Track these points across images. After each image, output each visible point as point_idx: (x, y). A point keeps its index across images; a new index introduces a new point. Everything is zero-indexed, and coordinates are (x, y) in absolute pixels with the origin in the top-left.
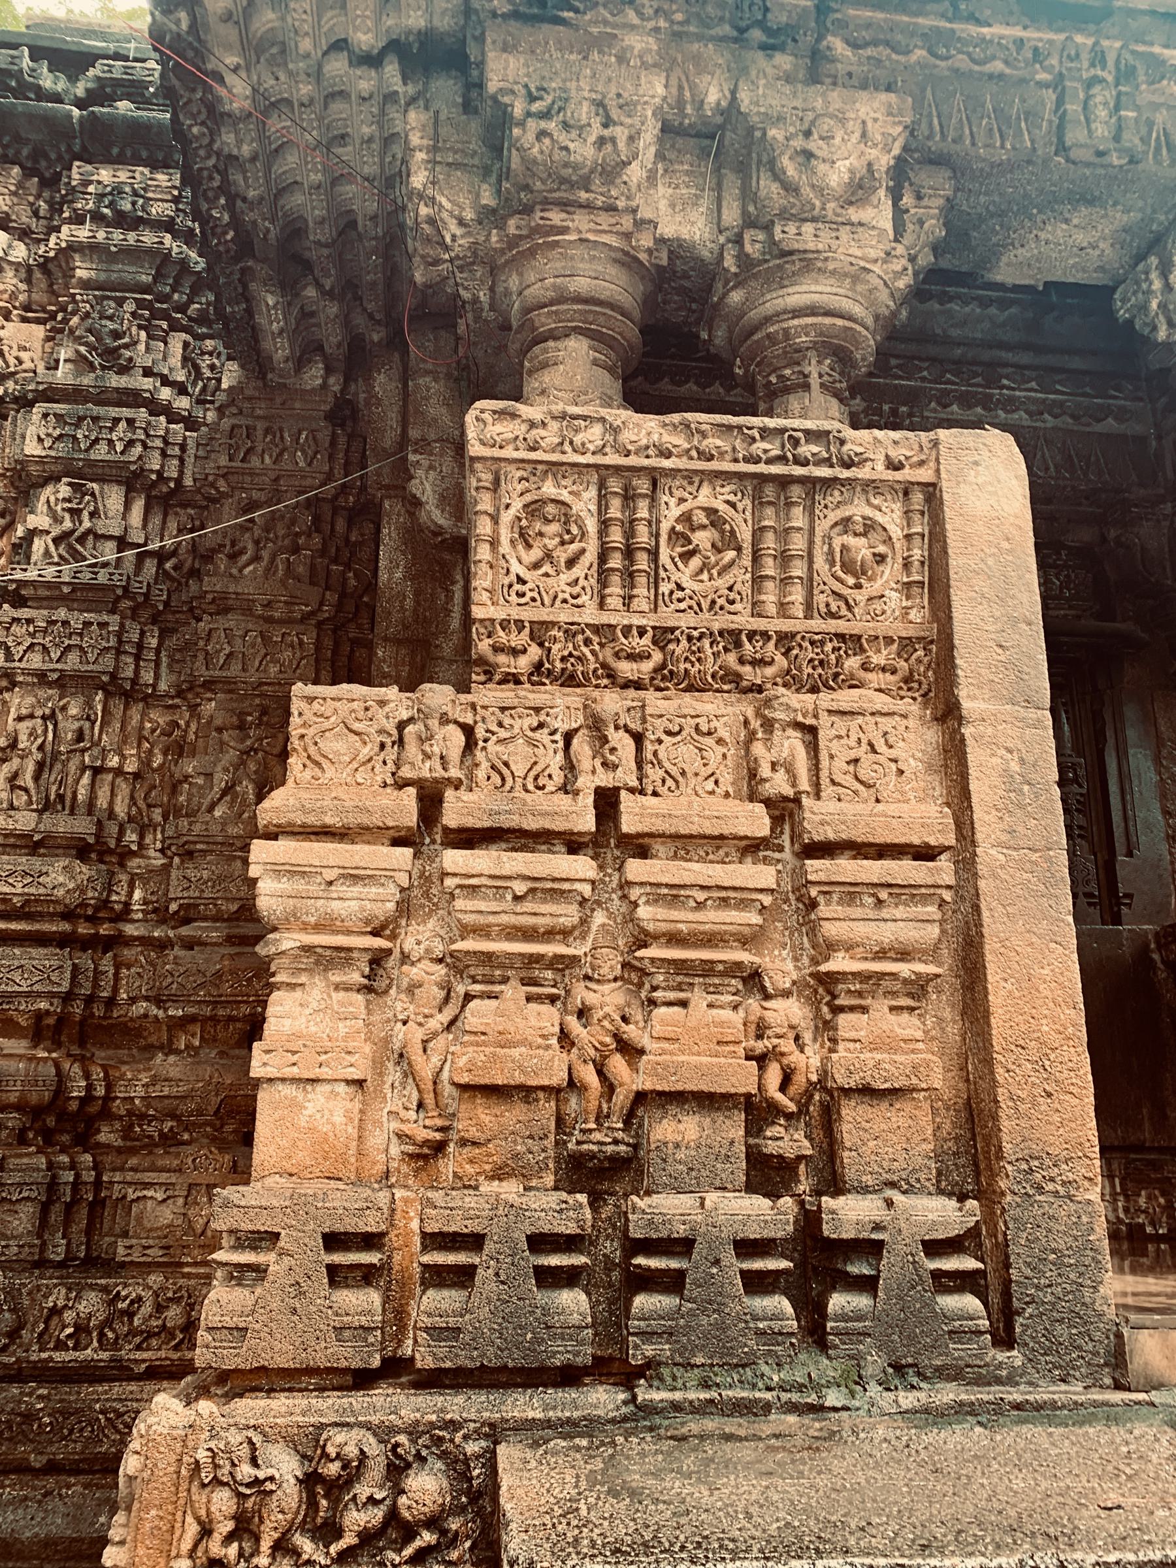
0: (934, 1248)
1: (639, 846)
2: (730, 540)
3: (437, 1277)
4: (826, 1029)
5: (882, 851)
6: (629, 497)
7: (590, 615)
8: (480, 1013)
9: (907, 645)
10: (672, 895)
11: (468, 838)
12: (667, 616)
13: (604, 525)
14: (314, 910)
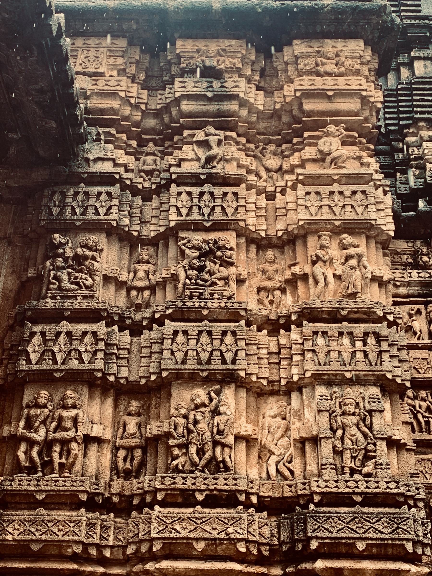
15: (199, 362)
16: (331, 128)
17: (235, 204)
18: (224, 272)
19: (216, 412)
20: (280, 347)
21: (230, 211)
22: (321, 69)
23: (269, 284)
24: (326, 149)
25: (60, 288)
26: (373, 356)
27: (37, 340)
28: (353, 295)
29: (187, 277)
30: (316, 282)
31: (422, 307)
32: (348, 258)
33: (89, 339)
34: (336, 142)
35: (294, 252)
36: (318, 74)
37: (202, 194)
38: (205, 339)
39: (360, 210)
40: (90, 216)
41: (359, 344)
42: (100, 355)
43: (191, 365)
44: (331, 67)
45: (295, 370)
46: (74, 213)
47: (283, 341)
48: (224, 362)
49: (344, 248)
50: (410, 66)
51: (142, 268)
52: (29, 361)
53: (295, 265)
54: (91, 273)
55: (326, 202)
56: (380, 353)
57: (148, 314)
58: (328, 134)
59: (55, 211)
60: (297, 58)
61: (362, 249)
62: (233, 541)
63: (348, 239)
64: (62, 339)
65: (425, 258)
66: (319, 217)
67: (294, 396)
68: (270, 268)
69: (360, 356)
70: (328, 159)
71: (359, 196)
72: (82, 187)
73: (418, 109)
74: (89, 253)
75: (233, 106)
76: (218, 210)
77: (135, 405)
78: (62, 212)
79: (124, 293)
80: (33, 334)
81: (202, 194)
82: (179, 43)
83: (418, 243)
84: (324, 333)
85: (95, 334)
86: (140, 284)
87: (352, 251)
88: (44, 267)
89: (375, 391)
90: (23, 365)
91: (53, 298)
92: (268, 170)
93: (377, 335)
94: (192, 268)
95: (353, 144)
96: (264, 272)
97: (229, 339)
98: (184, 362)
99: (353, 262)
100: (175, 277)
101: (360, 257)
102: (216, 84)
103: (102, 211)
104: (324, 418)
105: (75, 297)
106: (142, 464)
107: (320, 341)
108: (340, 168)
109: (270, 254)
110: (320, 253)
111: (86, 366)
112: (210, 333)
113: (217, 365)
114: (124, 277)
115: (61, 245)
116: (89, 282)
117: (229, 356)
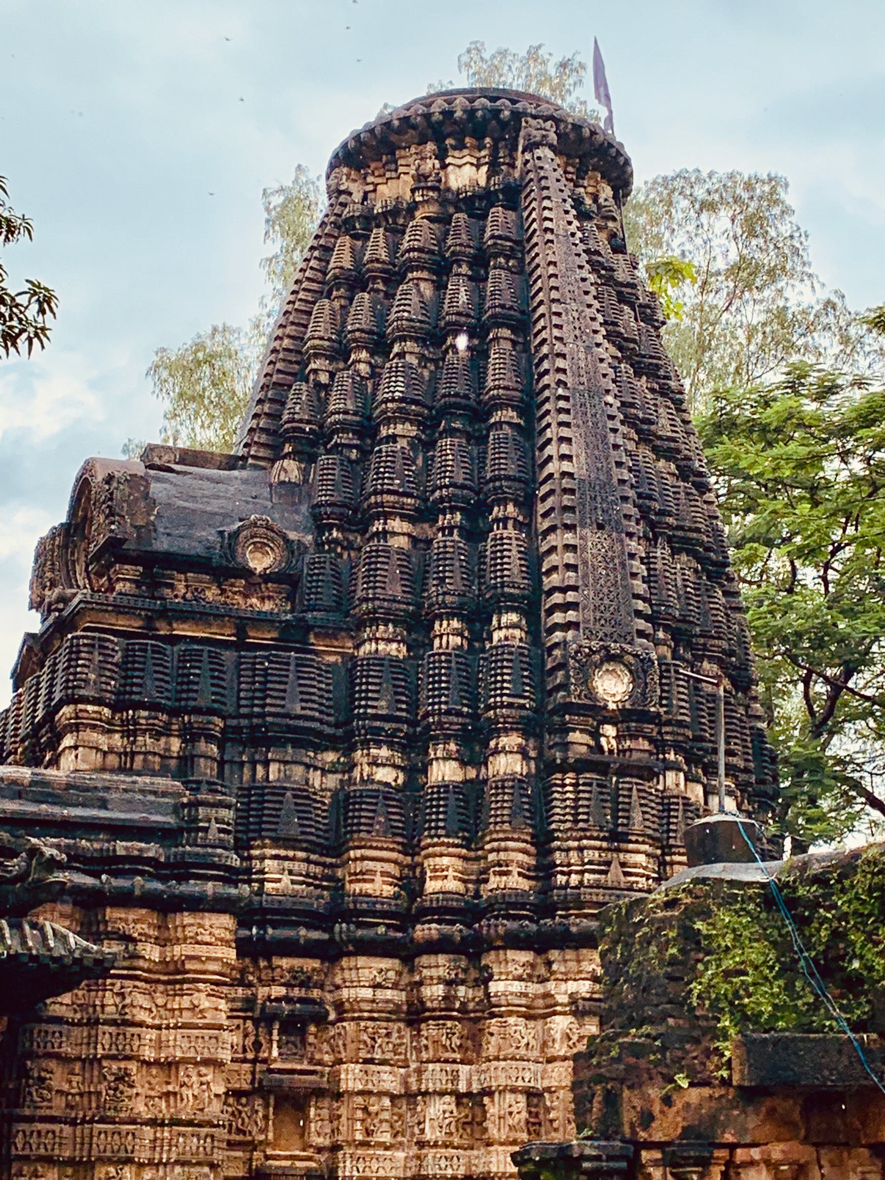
15: (113, 1152)
16: (201, 986)
17: (137, 1043)
20: (155, 1139)
21: (135, 1048)
22: (199, 938)
23: (153, 1093)
24: (196, 1002)
25: (32, 1101)
26: (208, 1149)
27: (21, 1134)
28: (202, 1110)
29: (107, 1094)
30: (182, 1100)
31: (241, 1021)
32: (202, 1084)
33: (50, 1135)
34: (203, 995)
35: (170, 1070)
36: (198, 943)
37: (118, 1034)
38: (116, 1137)
39: (212, 1050)
40: (49, 1049)
41: (202, 1142)
42: (56, 1146)
43: (108, 1154)
44: (207, 938)
45: (165, 1156)
46: (39, 1046)
47: (158, 1135)
48: (126, 1151)
49: (201, 1076)
50: (266, 764)
51: (76, 1079)
52: (17, 1149)
53: (168, 1083)
54: (50, 1090)
55: (193, 1044)
56: (213, 1148)
58: (199, 991)
59: (27, 1044)
60: (184, 927)
61: (209, 1078)
63: (203, 1070)
64: (35, 1134)
65: (251, 978)
66: (188, 1055)
67: (161, 1168)
68: (153, 1081)
69: (201, 1149)
70: (197, 1010)
71: (214, 1041)
72: (44, 1026)
73: (275, 678)
74: (48, 1076)
75: (141, 963)
76: (128, 1047)
78: (32, 1045)
79: (64, 1098)
80: (18, 1132)
81: (118, 1034)
82: (108, 910)
83: (247, 960)
84: (184, 1135)
85: (54, 1132)
86: (73, 1091)
87: (204, 1079)
88: (20, 1084)
89: (206, 1170)
91: (29, 1107)
92: (157, 1006)
93: (212, 1137)
94: (110, 1088)
95: (213, 995)
96: (150, 1083)
97: (130, 1137)
98: (105, 1151)
99: (205, 1087)
100: (99, 1094)
101: (208, 1083)
102: (131, 947)
103: (56, 1045)
105: (41, 1108)
107: (181, 1140)
108: (205, 1017)
109: (154, 1071)
110: (186, 1080)
111: (49, 1153)
112: (119, 1133)
113: (123, 1154)
114: (66, 1087)
115: (31, 1069)
116: (49, 1097)
117: (130, 1148)
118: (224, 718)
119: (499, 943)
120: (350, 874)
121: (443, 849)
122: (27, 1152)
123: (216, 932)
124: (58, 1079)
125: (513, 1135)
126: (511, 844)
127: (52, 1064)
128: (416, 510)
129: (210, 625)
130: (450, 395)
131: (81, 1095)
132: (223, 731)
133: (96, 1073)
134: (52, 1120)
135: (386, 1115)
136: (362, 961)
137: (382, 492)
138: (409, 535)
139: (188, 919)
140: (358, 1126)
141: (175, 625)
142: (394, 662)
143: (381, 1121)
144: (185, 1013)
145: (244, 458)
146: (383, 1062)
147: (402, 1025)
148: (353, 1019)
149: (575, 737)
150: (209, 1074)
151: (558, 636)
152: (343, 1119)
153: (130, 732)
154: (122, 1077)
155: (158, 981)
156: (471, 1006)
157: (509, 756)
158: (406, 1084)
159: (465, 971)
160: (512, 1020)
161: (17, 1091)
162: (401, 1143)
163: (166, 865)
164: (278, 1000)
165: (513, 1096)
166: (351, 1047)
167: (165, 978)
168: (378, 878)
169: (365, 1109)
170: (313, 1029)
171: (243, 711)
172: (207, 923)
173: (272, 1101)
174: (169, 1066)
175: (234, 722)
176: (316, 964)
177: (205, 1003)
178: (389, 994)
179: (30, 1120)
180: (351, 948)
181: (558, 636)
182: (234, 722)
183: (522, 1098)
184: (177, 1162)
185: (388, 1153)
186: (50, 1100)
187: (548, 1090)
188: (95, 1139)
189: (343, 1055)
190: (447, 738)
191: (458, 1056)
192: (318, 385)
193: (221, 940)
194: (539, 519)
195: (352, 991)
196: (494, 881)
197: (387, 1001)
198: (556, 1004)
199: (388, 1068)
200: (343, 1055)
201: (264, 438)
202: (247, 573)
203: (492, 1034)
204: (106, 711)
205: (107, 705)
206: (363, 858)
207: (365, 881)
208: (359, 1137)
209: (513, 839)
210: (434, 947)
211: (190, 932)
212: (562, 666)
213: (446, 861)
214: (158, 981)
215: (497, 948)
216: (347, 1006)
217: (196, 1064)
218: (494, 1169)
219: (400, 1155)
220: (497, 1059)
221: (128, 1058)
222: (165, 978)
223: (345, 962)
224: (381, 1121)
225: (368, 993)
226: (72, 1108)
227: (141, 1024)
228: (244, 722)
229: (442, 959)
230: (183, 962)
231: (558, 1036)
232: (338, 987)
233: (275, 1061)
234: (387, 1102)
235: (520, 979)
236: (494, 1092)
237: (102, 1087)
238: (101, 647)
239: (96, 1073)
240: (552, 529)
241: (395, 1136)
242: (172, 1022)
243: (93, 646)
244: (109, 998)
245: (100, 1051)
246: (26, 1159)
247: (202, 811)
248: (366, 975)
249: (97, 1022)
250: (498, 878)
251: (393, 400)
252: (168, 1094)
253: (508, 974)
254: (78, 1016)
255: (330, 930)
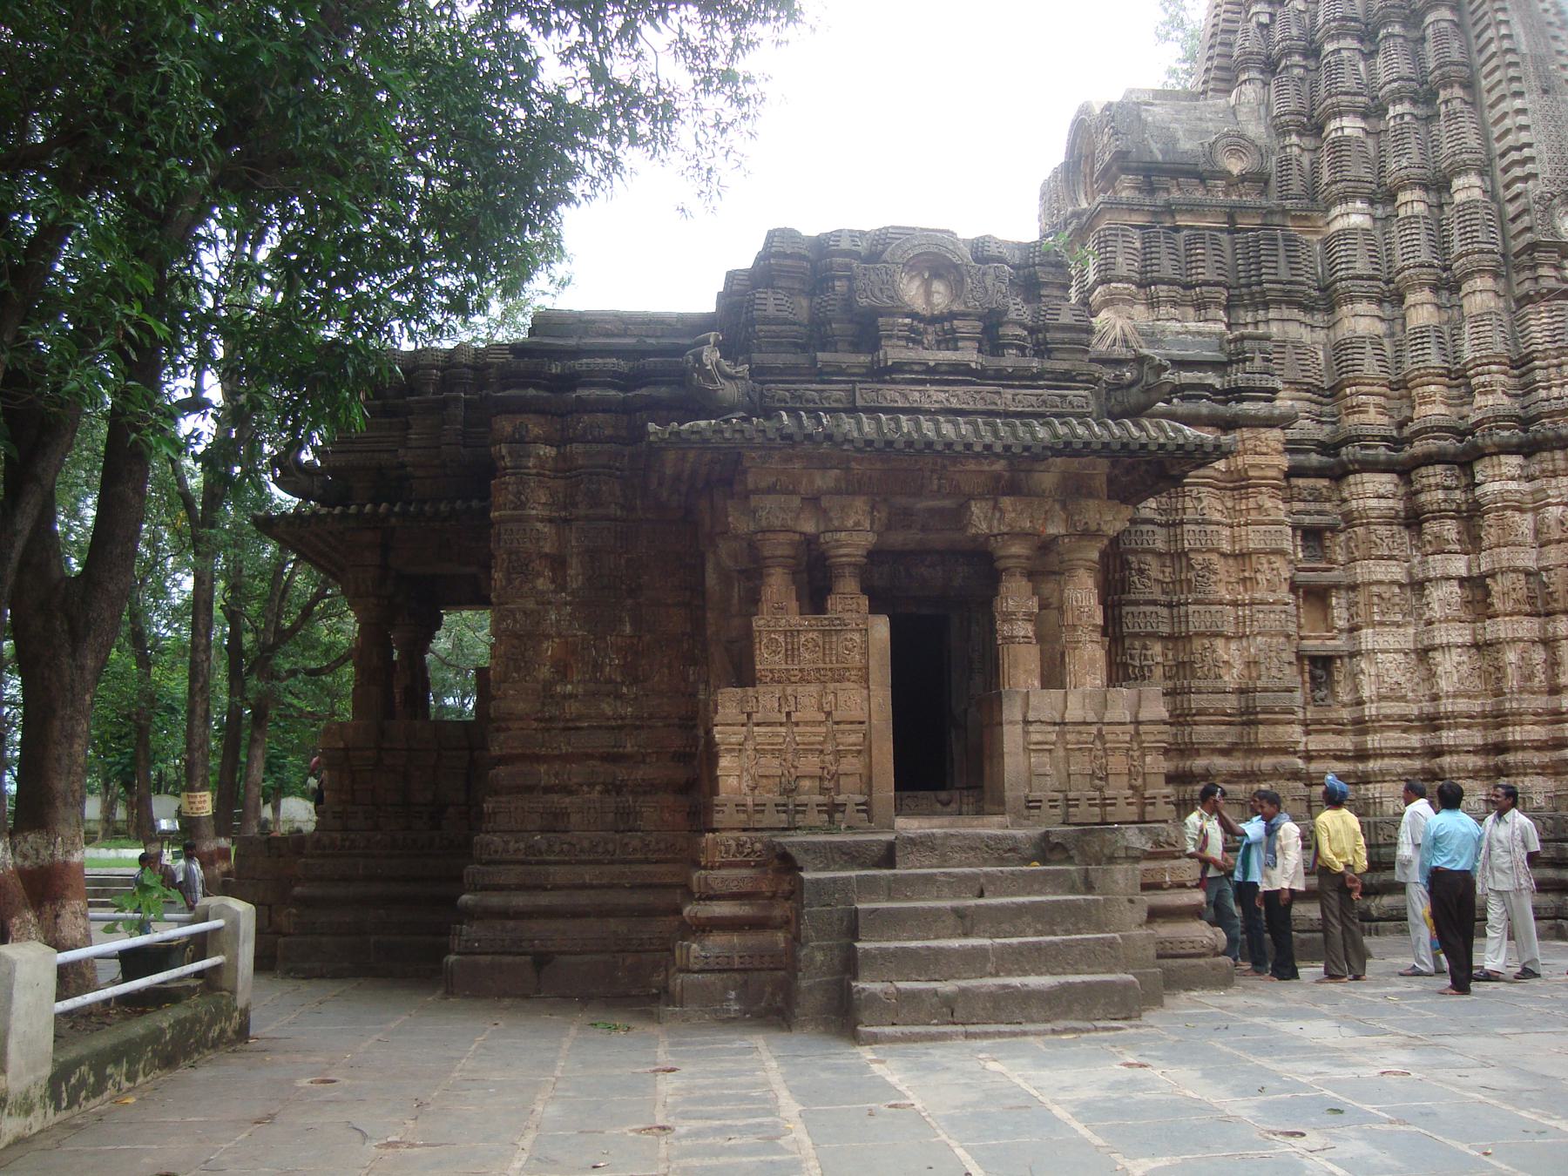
0: (857, 805)
1: (797, 724)
2: (817, 645)
3: (758, 812)
4: (837, 761)
5: (852, 723)
6: (792, 635)
7: (784, 667)
8: (762, 761)
9: (860, 669)
10: (802, 734)
11: (758, 725)
12: (802, 666)
13: (786, 643)
14: (727, 741)
16: (1264, 489)
18: (1214, 578)
19: (1214, 651)
23: (1232, 580)
34: (1265, 497)
36: (1256, 453)
38: (1208, 615)
43: (1203, 629)
44: (1264, 450)
51: (1168, 570)
57: (1175, 599)
58: (1261, 493)
62: (1224, 709)
63: (1273, 558)
77: (1170, 646)
86: (1167, 580)
87: (1275, 566)
89: (1282, 639)
90: (1125, 629)
104: (1262, 655)
106: (1177, 672)
114: (1161, 577)
118: (1228, 288)
119: (1493, 450)
120: (1347, 408)
121: (1430, 379)
122: (1137, 630)
123: (1272, 444)
124: (1154, 568)
125: (1518, 607)
126: (1494, 368)
127: (1149, 558)
128: (1366, 107)
129: (1205, 216)
130: (1386, 6)
131: (1173, 582)
132: (1228, 299)
133: (1184, 564)
134: (1154, 603)
135: (1397, 600)
136: (1366, 476)
137: (1336, 95)
138: (1363, 129)
139: (1246, 433)
140: (1375, 609)
141: (1178, 218)
142: (1366, 231)
143: (1394, 605)
144: (1252, 512)
145: (1204, 92)
146: (1391, 558)
147: (1402, 528)
148: (1362, 524)
149: (1542, 271)
150: (1279, 562)
151: (1518, 187)
152: (1361, 606)
153: (1153, 303)
154: (1207, 567)
155: (1225, 488)
156: (1464, 507)
157: (1484, 294)
158: (1410, 574)
159: (1457, 478)
160: (1509, 513)
161: (1123, 580)
162: (1409, 623)
163: (1225, 392)
164: (1298, 512)
165: (1514, 575)
166: (1362, 547)
167: (1231, 485)
168: (1372, 410)
169: (1379, 596)
170: (1328, 534)
171: (1242, 281)
172: (1263, 436)
173: (1301, 593)
174: (1241, 556)
175: (1237, 292)
176: (1326, 482)
177: (1268, 504)
178: (1391, 503)
179: (1136, 603)
180: (1357, 467)
181: (1518, 187)
182: (1237, 292)
183: (1522, 577)
184: (1259, 633)
185: (1402, 630)
186: (1150, 587)
187: (1547, 569)
188: (1190, 618)
189: (1356, 554)
190: (1422, 285)
191: (1457, 547)
192: (1261, 25)
193: (1275, 450)
194: (1485, 95)
195: (1361, 501)
196: (1480, 400)
197: (1392, 509)
198: (1549, 497)
199: (1395, 562)
200: (1356, 554)
201: (1220, 74)
202: (1226, 175)
203: (1490, 526)
204: (1134, 287)
205: (1134, 283)
206: (1358, 393)
207: (1361, 412)
208: (1377, 618)
209: (1495, 363)
210: (1430, 459)
211: (1250, 444)
212: (1526, 211)
213: (1433, 388)
214: (1225, 488)
215: (1491, 455)
216: (1356, 514)
217: (1267, 553)
218: (1503, 636)
219: (1411, 630)
220: (1498, 546)
221: (1210, 551)
222: (1231, 485)
223: (1351, 479)
224: (1394, 605)
225: (1373, 503)
226: (1167, 593)
227: (1218, 524)
228: (1244, 290)
229: (1439, 468)
230: (1246, 470)
231: (1553, 523)
232: (1344, 501)
233: (1300, 561)
234: (1397, 590)
235: (1512, 479)
236: (1496, 573)
237: (1191, 575)
238: (1123, 236)
239: (1184, 564)
240: (1502, 98)
241: (1404, 616)
242: (1242, 520)
243: (1117, 235)
244: (1189, 503)
245: (1186, 545)
246: (1136, 636)
247: (1247, 344)
248: (1369, 487)
249: (1182, 523)
250: (1484, 397)
251: (1335, 20)
252: (1244, 580)
253: (1501, 476)
254: (1164, 518)
255: (1338, 455)
